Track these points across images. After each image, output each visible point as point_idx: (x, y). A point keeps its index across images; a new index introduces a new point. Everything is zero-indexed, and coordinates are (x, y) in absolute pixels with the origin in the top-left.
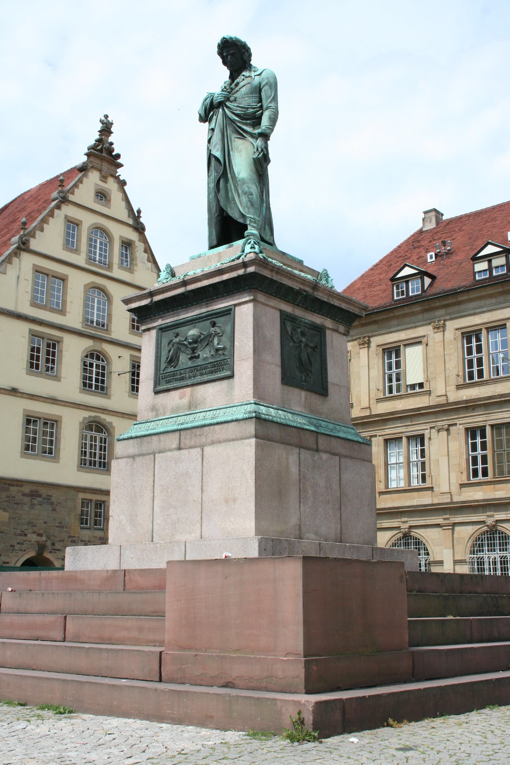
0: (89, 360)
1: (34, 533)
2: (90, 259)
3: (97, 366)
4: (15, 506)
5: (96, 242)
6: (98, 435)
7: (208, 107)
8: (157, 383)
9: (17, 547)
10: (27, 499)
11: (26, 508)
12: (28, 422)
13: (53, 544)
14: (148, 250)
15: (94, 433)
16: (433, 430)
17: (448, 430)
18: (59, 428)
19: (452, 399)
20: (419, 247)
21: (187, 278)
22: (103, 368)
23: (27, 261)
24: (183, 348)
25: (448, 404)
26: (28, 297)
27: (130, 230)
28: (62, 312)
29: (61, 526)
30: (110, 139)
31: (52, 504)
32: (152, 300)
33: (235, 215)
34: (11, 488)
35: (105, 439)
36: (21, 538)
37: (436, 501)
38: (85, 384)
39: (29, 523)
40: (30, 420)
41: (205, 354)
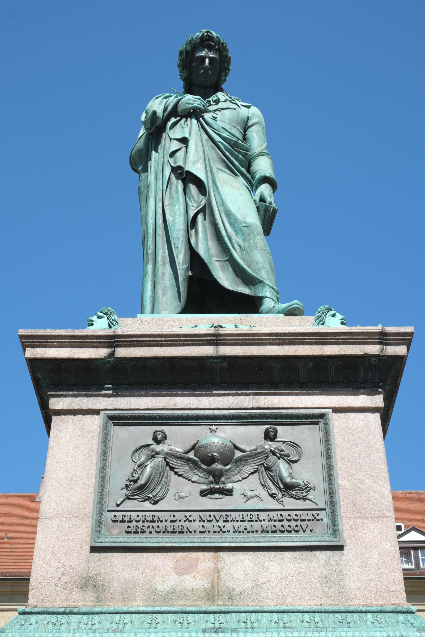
7: (170, 108)
21: (221, 331)
24: (182, 468)
32: (112, 354)
33: (226, 279)
41: (247, 489)
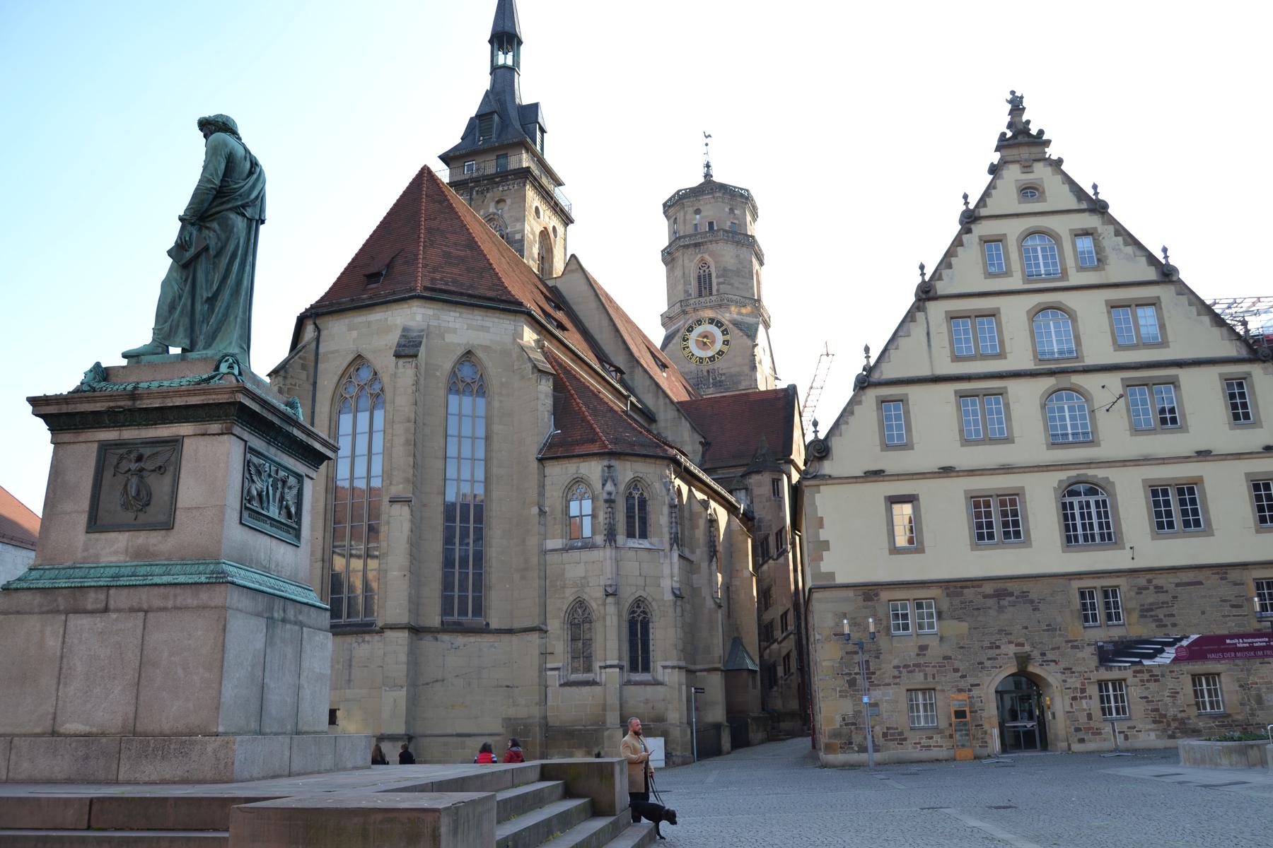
1: (1010, 642)
2: (1028, 277)
4: (976, 613)
5: (1035, 250)
6: (1092, 500)
10: (991, 602)
11: (992, 613)
12: (977, 505)
13: (1043, 654)
14: (1121, 231)
15: (1083, 498)
18: (1024, 503)
23: (936, 310)
26: (947, 352)
27: (1086, 215)
28: (1002, 355)
29: (1051, 629)
30: (1024, 118)
31: (1032, 602)
34: (965, 591)
35: (1104, 502)
36: (991, 651)
39: (1000, 631)
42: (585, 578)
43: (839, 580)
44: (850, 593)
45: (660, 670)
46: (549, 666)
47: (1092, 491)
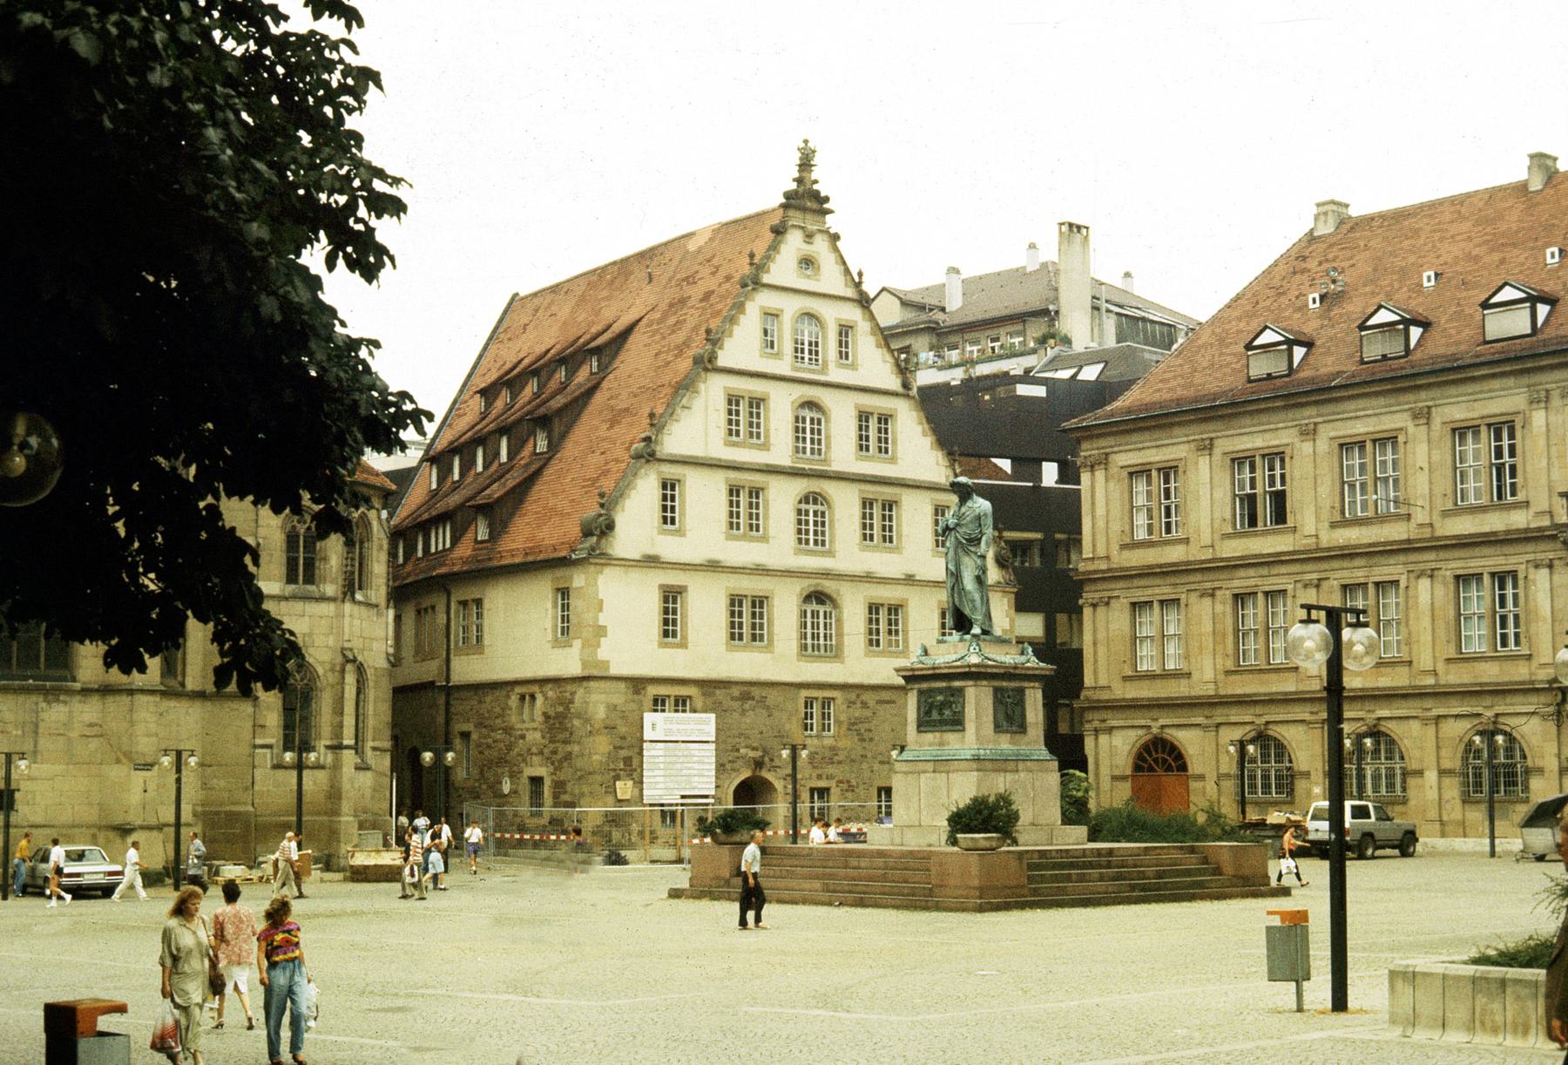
0: (803, 506)
3: (815, 514)
6: (822, 609)
8: (919, 726)
9: (728, 766)
10: (736, 704)
11: (736, 715)
16: (1299, 585)
17: (1318, 586)
19: (1324, 543)
20: (1303, 271)
22: (823, 514)
25: (1318, 549)
28: (765, 447)
31: (768, 708)
37: (1301, 688)
38: (800, 540)
40: (735, 601)
41: (947, 712)
42: (310, 635)
43: (613, 671)
44: (622, 685)
45: (369, 753)
46: (259, 741)
47: (821, 602)
